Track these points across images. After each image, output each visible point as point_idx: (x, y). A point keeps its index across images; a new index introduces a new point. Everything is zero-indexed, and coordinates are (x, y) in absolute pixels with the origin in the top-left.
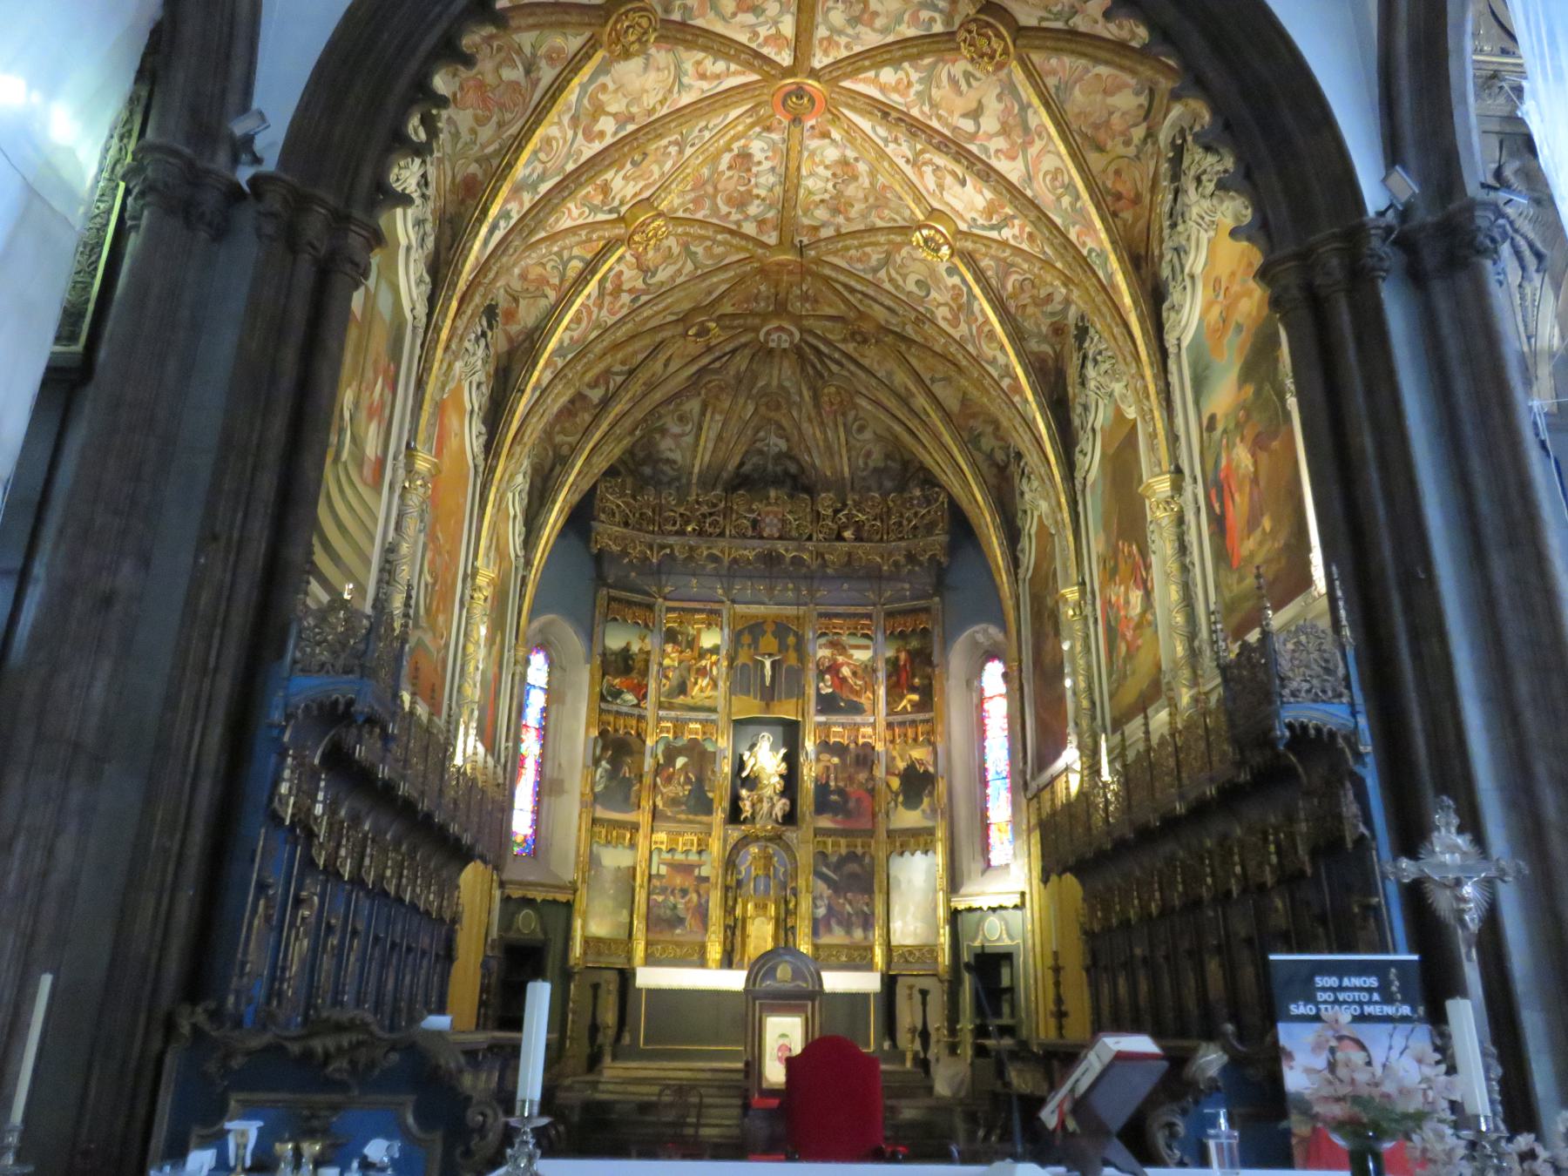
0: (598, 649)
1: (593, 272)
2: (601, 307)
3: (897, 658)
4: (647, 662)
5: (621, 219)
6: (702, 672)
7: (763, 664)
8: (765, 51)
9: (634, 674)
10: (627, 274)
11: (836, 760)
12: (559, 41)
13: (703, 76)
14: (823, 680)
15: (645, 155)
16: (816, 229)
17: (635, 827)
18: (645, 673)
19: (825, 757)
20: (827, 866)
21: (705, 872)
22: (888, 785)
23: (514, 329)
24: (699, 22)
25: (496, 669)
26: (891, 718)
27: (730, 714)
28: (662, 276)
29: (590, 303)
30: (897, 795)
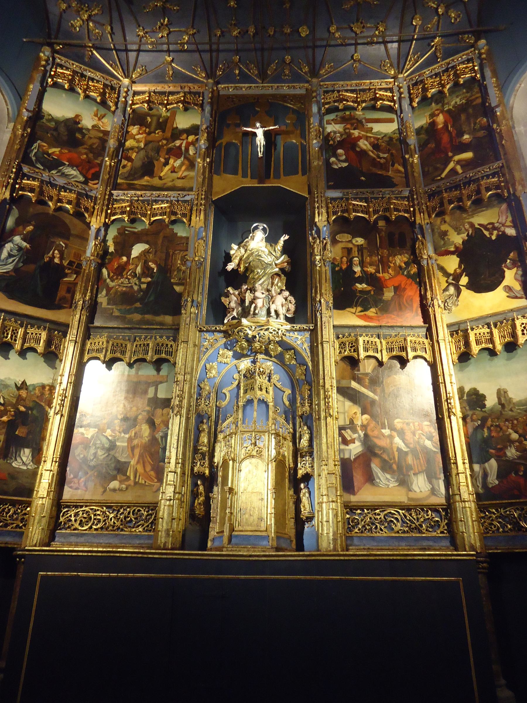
0: (30, 102)
3: (433, 124)
4: (103, 141)
6: (177, 153)
7: (255, 135)
9: (82, 149)
11: (360, 241)
14: (335, 155)
17: (63, 329)
19: (343, 238)
20: (359, 380)
21: (161, 395)
22: (442, 269)
26: (434, 187)
27: (209, 191)
30: (457, 277)
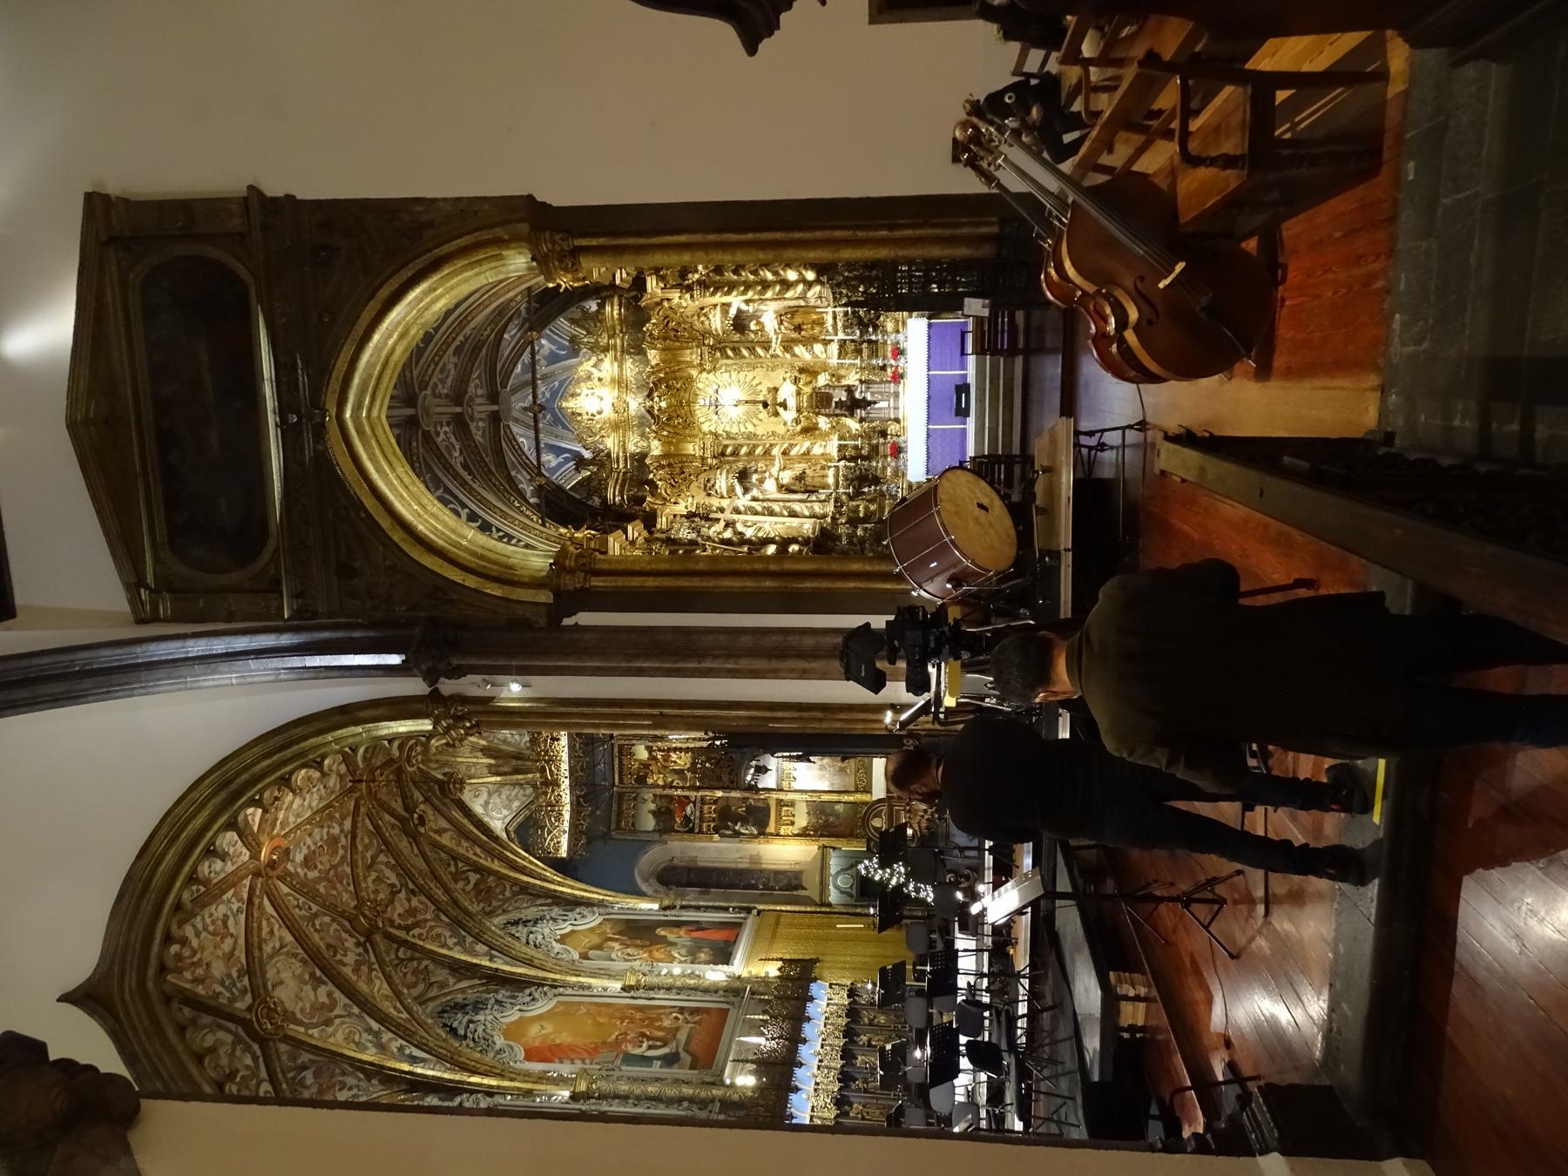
1: (407, 942)
2: (426, 921)
4: (661, 797)
5: (369, 939)
8: (245, 896)
10: (400, 910)
12: (284, 1058)
13: (271, 932)
15: (329, 946)
16: (341, 777)
17: (780, 803)
18: (670, 798)
23: (452, 981)
24: (243, 960)
25: (682, 932)
28: (393, 879)
29: (424, 931)
